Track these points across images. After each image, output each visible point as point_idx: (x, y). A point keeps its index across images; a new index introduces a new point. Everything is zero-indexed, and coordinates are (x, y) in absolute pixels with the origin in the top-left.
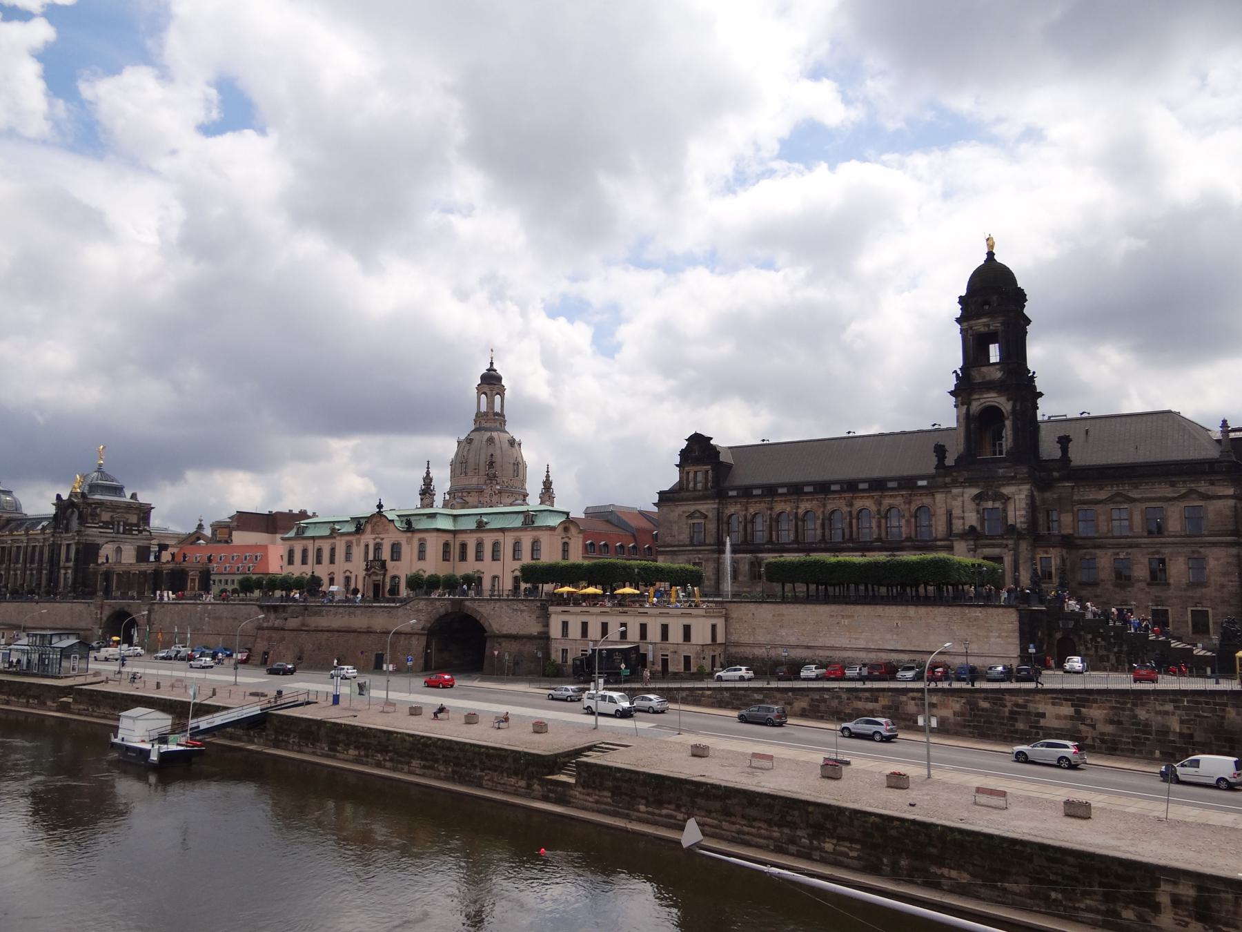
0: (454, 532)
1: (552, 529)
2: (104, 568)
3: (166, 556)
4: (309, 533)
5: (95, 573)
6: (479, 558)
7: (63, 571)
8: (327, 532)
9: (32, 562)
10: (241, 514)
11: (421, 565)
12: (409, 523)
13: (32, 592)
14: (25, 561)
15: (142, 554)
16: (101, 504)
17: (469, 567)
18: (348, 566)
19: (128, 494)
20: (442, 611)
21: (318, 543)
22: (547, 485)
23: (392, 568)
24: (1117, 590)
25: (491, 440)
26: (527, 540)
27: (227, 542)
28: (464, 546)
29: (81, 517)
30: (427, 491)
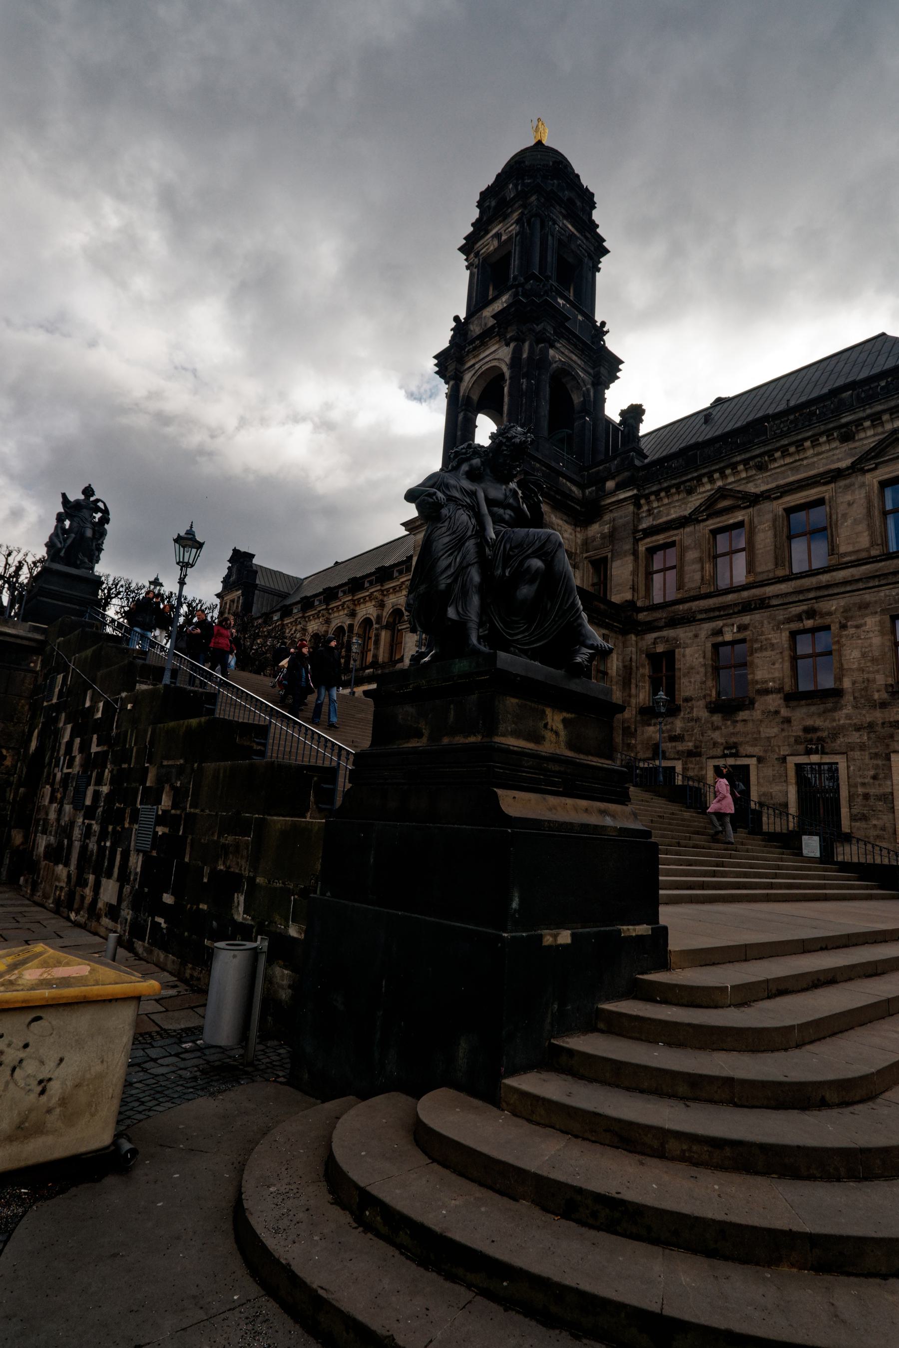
24: (717, 718)
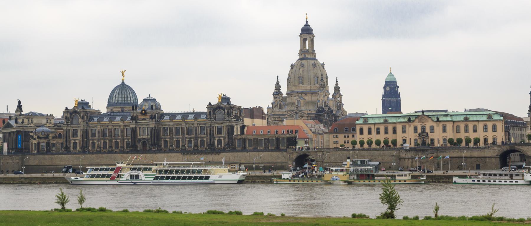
0: (454, 122)
1: (500, 120)
2: (239, 137)
4: (370, 121)
6: (466, 131)
7: (217, 139)
8: (382, 121)
11: (445, 134)
12: (438, 119)
14: (184, 134)
17: (462, 135)
18: (404, 135)
20: (505, 149)
21: (377, 126)
22: (337, 89)
23: (431, 136)
25: (315, 65)
26: (490, 125)
28: (458, 128)
29: (229, 114)
30: (277, 92)
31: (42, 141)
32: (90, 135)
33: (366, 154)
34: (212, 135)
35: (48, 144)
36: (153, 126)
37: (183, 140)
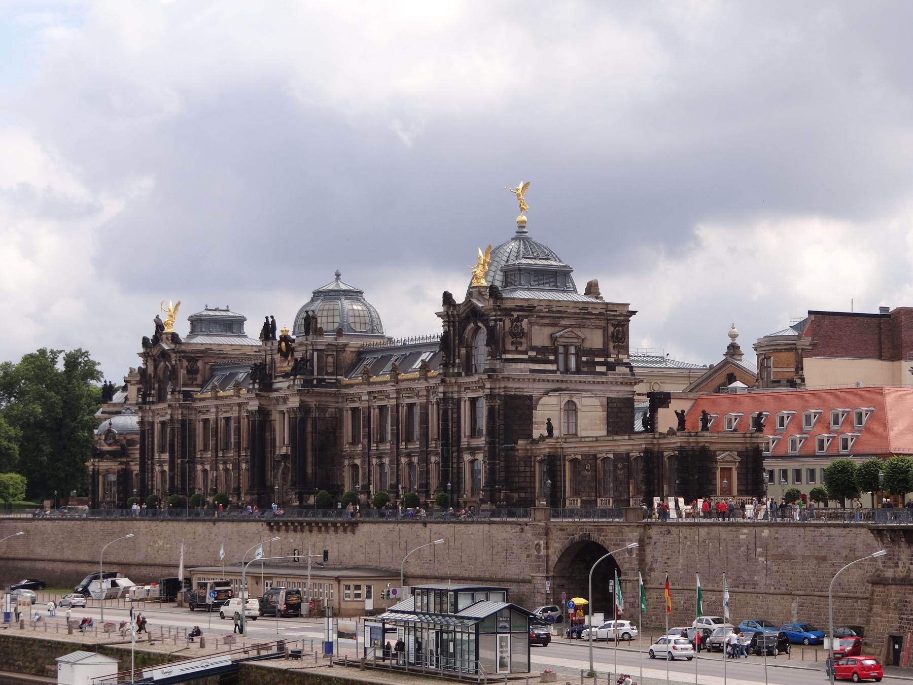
2: (544, 449)
3: (666, 419)
5: (529, 460)
7: (467, 457)
9: (409, 439)
10: (818, 317)
13: (412, 502)
14: (396, 435)
15: (619, 415)
16: (529, 309)
19: (581, 288)
27: (792, 383)
29: (492, 340)
31: (104, 465)
32: (200, 444)
33: (800, 550)
34: (449, 437)
35: (124, 475)
36: (294, 402)
37: (391, 462)
